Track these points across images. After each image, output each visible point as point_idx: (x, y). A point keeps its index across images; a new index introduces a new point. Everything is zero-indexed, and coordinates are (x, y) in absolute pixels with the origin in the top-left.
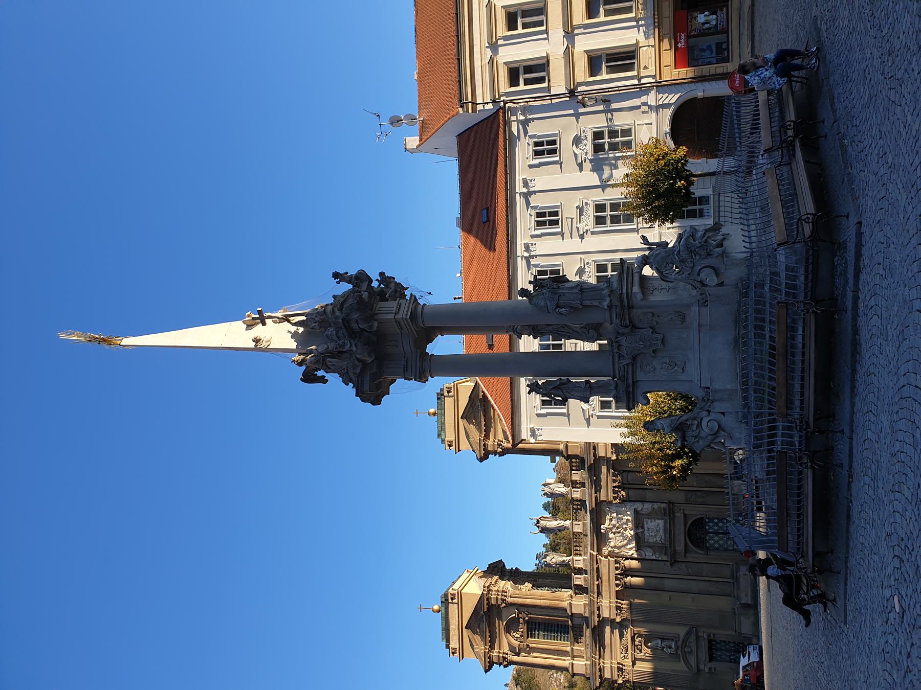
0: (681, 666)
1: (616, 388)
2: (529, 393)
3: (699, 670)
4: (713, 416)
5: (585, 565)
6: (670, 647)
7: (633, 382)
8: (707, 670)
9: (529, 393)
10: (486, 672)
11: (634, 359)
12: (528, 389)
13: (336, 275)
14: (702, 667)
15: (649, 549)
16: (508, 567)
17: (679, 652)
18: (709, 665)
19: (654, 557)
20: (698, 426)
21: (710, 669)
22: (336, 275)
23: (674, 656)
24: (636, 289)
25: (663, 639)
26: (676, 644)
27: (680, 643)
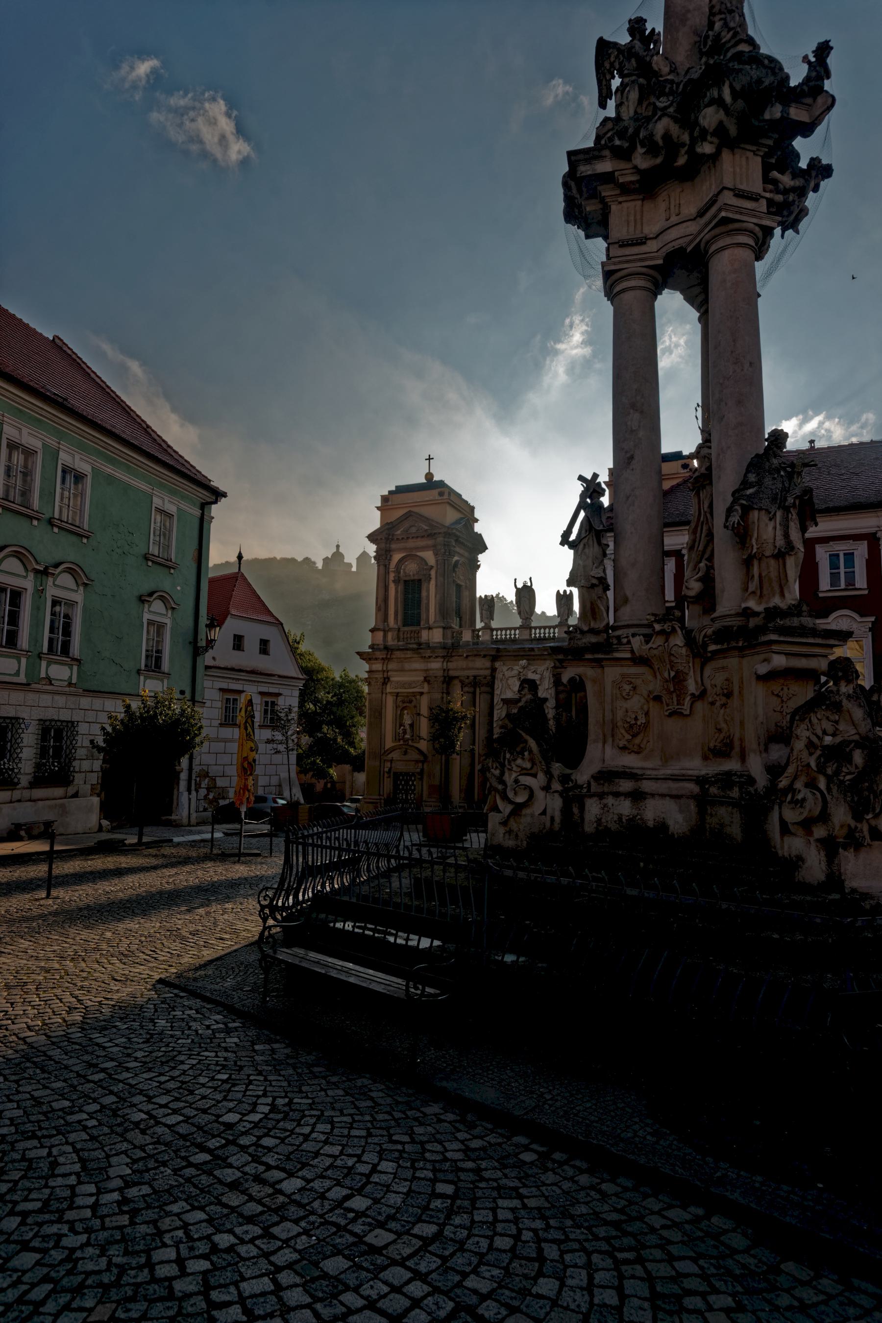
1: (592, 631)
2: (581, 478)
4: (540, 795)
5: (482, 643)
7: (602, 660)
9: (581, 478)
12: (589, 477)
13: (824, 50)
16: (481, 557)
19: (495, 719)
20: (523, 769)
22: (824, 50)
23: (396, 738)
24: (779, 661)
25: (412, 726)
26: (408, 740)
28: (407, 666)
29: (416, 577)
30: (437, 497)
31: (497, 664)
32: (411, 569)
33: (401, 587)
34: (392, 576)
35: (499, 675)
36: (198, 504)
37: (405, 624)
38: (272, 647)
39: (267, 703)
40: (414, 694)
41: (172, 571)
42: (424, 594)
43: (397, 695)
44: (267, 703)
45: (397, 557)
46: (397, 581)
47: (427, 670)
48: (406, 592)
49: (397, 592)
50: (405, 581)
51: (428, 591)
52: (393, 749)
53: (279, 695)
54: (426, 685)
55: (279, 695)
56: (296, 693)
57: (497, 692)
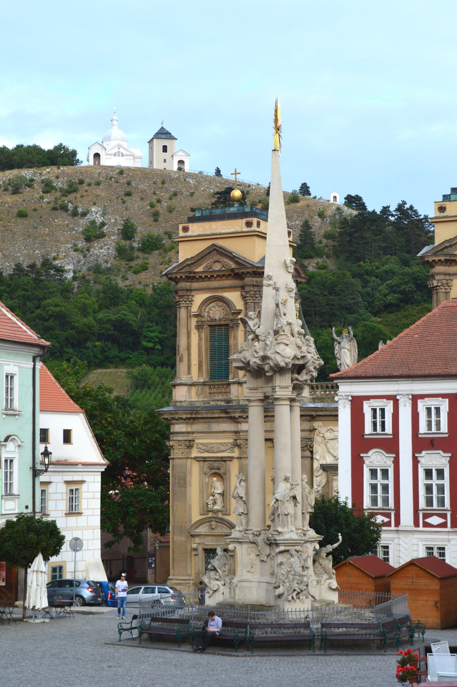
0: (196, 516)
3: (192, 536)
6: (215, 503)
7: (241, 542)
8: (194, 546)
10: (217, 168)
11: (254, 543)
14: (197, 540)
15: (324, 481)
17: (210, 515)
18: (200, 549)
21: (196, 550)
23: (206, 510)
25: (222, 495)
26: (218, 511)
27: (220, 515)
28: (216, 427)
29: (222, 323)
30: (245, 229)
31: (316, 424)
32: (216, 313)
33: (205, 333)
34: (194, 321)
35: (318, 439)
36: (31, 359)
37: (212, 377)
38: (74, 437)
39: (71, 491)
40: (223, 460)
41: (17, 417)
42: (232, 342)
43: (204, 460)
44: (71, 491)
45: (199, 298)
46: (199, 327)
47: (236, 432)
48: (212, 338)
49: (200, 339)
50: (210, 326)
51: (235, 338)
52: (200, 523)
53: (82, 482)
54: (236, 450)
55: (82, 482)
56: (98, 478)
57: (316, 456)
